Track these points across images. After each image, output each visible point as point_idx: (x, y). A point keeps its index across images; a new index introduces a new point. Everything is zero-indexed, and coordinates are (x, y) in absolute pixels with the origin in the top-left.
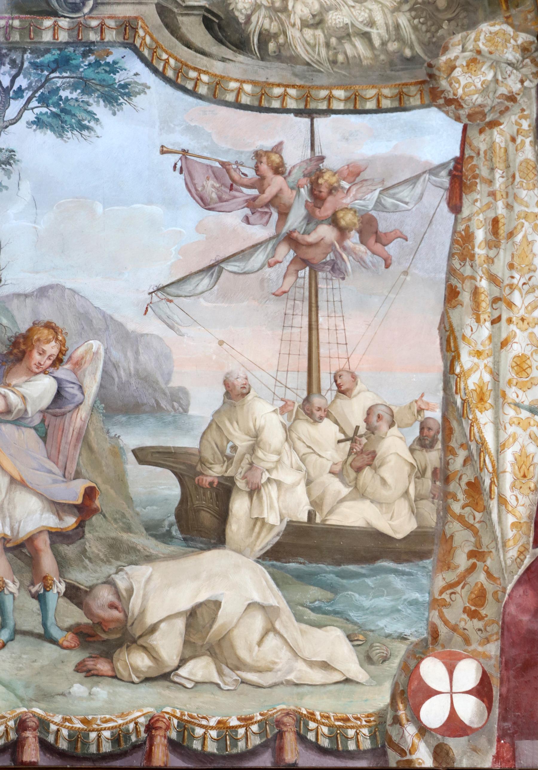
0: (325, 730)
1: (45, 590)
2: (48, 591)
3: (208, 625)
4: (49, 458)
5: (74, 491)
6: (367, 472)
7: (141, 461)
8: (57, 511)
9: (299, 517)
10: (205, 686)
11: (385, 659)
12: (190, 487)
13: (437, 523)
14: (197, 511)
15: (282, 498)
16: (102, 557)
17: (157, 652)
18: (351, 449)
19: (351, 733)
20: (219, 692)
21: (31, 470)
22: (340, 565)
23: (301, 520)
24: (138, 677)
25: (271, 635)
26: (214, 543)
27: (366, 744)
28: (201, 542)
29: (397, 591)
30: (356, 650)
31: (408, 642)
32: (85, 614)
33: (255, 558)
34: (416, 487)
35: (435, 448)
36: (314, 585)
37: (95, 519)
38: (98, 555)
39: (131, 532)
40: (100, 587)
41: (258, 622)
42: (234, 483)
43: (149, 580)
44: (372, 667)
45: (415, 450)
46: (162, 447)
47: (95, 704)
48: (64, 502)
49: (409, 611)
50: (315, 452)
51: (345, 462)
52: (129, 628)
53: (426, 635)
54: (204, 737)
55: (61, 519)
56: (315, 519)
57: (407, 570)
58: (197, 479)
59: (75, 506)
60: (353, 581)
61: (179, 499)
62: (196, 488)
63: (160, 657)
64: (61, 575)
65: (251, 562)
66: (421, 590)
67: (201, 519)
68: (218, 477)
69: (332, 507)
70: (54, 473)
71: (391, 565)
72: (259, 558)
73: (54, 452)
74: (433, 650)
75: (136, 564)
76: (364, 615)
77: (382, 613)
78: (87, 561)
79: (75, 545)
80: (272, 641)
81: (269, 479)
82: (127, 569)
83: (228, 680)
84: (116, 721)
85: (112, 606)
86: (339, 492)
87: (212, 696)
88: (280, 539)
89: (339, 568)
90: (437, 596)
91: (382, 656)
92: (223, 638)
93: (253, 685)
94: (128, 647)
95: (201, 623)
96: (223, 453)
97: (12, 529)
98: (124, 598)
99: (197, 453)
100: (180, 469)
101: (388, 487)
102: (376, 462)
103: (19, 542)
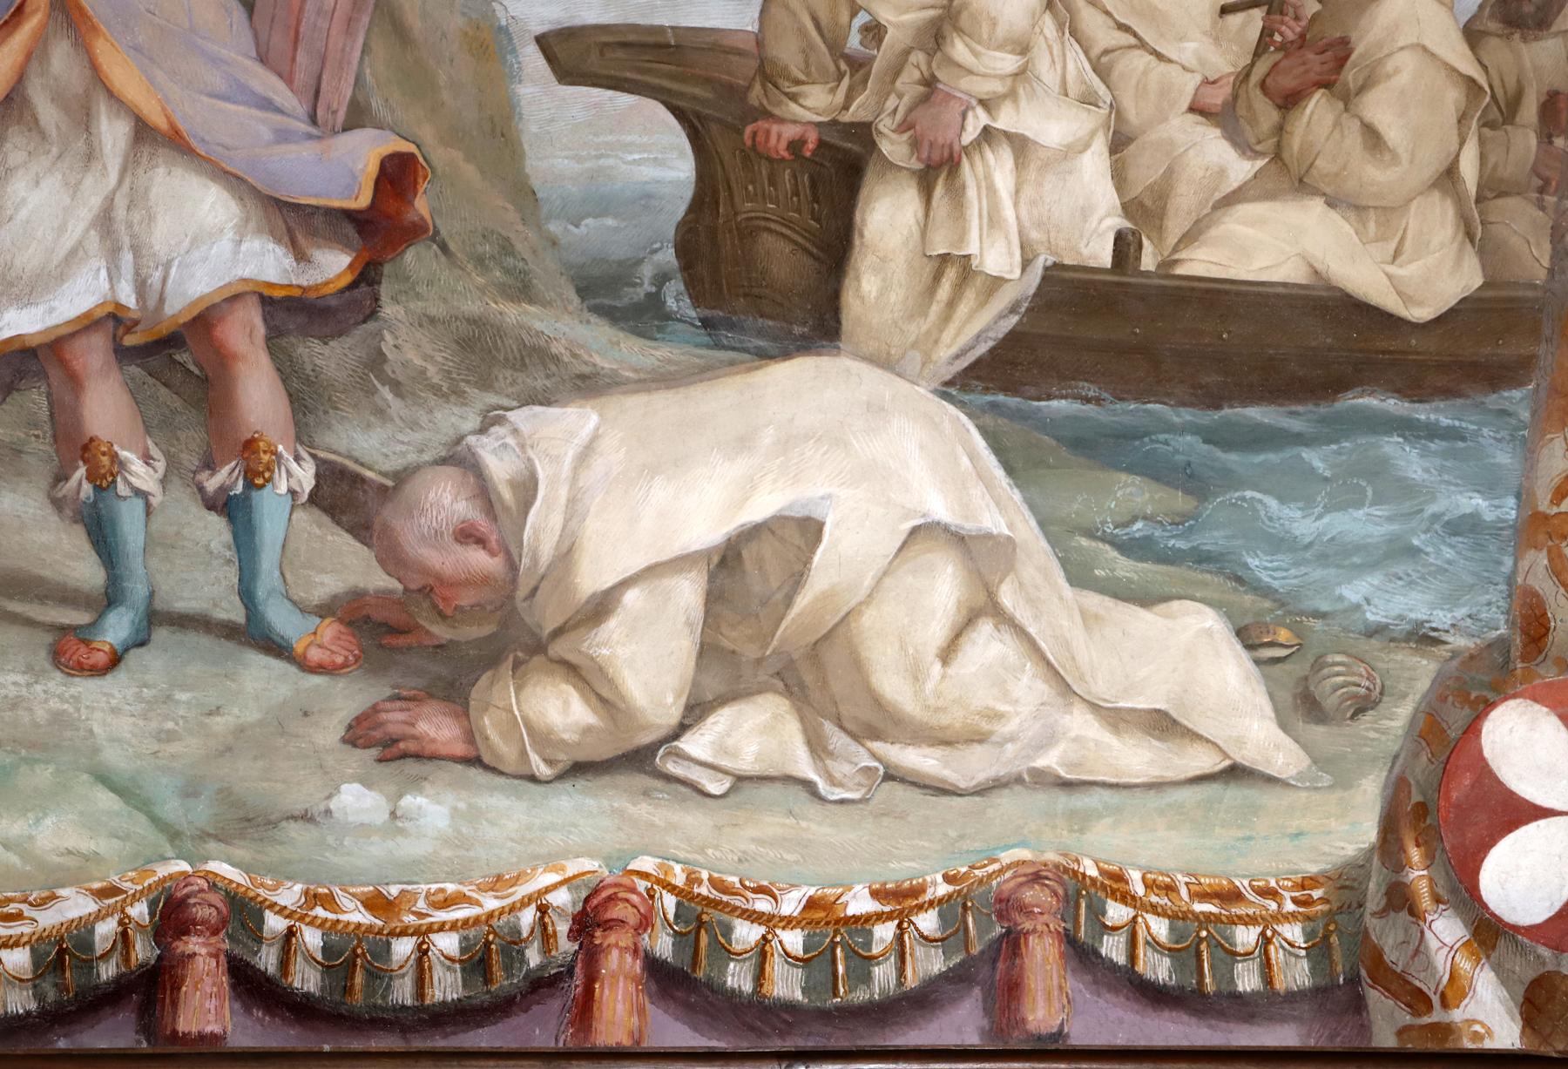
0: (1160, 928)
1: (250, 485)
2: (262, 487)
3: (779, 596)
4: (263, 59)
5: (347, 168)
6: (1318, 108)
7: (567, 73)
8: (290, 231)
9: (1086, 252)
10: (767, 791)
11: (1363, 705)
12: (727, 157)
13: (1551, 271)
14: (748, 233)
15: (1028, 192)
16: (436, 380)
17: (611, 682)
18: (1266, 33)
19: (1246, 937)
20: (814, 809)
21: (205, 99)
22: (1218, 407)
23: (1092, 264)
24: (549, 762)
25: (986, 627)
26: (803, 336)
27: (1296, 974)
28: (760, 333)
29: (1407, 489)
30: (1266, 677)
31: (1442, 651)
32: (382, 562)
33: (935, 385)
34: (1483, 158)
35: (1554, 29)
36: (1130, 470)
37: (415, 258)
38: (423, 372)
39: (531, 302)
40: (428, 474)
41: (942, 587)
42: (873, 146)
43: (586, 454)
44: (1318, 732)
45: (1485, 33)
46: (635, 28)
47: (410, 848)
48: (313, 201)
49: (1448, 553)
50: (1142, 45)
51: (1245, 75)
52: (521, 605)
53: (1503, 630)
54: (762, 952)
55: (301, 256)
56: (1138, 259)
57: (1445, 421)
58: (748, 130)
59: (349, 215)
60: (1259, 458)
61: (688, 193)
62: (746, 159)
63: (623, 698)
64: (303, 435)
65: (922, 395)
66: (1489, 485)
67: (761, 257)
68: (818, 124)
69: (1197, 222)
70: (279, 111)
71: (1393, 405)
72: (948, 384)
73: (279, 42)
74: (1528, 676)
75: (547, 403)
76: (1297, 564)
77: (1356, 560)
78: (386, 392)
79: (348, 341)
80: (988, 647)
81: (986, 130)
82: (517, 417)
83: (841, 769)
84: (478, 903)
85: (467, 535)
86: (1222, 172)
87: (791, 821)
88: (1020, 323)
89: (1216, 415)
90: (1544, 506)
91: (1355, 696)
92: (828, 636)
93: (925, 787)
94: (517, 665)
95: (757, 588)
96: (835, 46)
97: (141, 287)
98: (507, 509)
99: (751, 46)
100: (695, 98)
101: (1387, 157)
102: (1350, 76)
103: (164, 330)
